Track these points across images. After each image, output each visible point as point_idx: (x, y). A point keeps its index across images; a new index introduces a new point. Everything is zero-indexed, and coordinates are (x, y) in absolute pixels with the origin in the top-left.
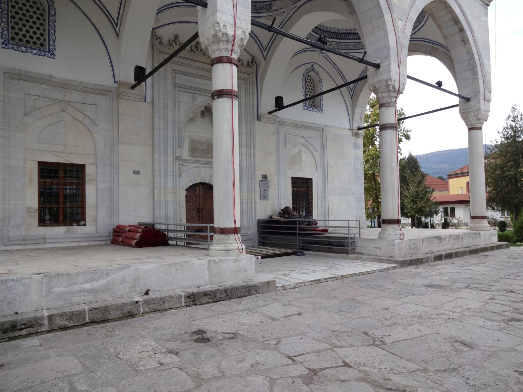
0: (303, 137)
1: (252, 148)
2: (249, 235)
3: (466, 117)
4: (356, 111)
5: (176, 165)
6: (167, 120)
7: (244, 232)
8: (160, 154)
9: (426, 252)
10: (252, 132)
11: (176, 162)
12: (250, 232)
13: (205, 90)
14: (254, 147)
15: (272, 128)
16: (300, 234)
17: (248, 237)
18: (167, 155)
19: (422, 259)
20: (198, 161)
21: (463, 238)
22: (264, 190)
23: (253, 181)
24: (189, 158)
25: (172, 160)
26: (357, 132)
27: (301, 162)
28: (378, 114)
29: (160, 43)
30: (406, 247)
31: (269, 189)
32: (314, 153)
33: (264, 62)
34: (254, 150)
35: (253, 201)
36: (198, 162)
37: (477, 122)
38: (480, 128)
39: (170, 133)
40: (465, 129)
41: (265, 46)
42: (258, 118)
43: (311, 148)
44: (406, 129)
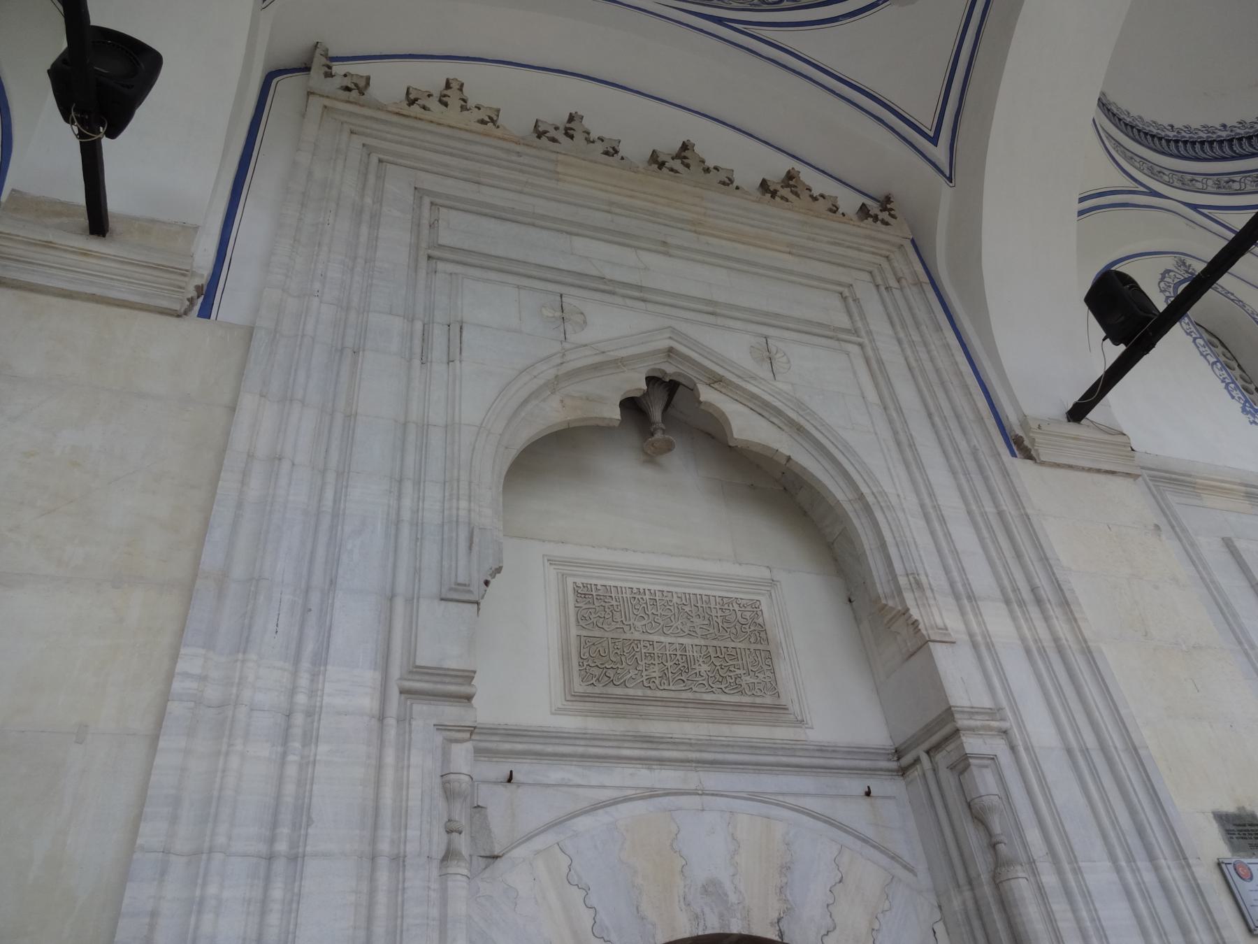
1: (1055, 612)
5: (404, 747)
6: (351, 417)
8: (243, 642)
11: (404, 720)
13: (640, 288)
18: (321, 660)
20: (649, 740)
23: (1173, 874)
24: (570, 723)
25: (368, 702)
29: (348, 89)
33: (946, 191)
34: (1072, 619)
36: (652, 752)
39: (367, 496)
41: (928, 122)
42: (1019, 446)
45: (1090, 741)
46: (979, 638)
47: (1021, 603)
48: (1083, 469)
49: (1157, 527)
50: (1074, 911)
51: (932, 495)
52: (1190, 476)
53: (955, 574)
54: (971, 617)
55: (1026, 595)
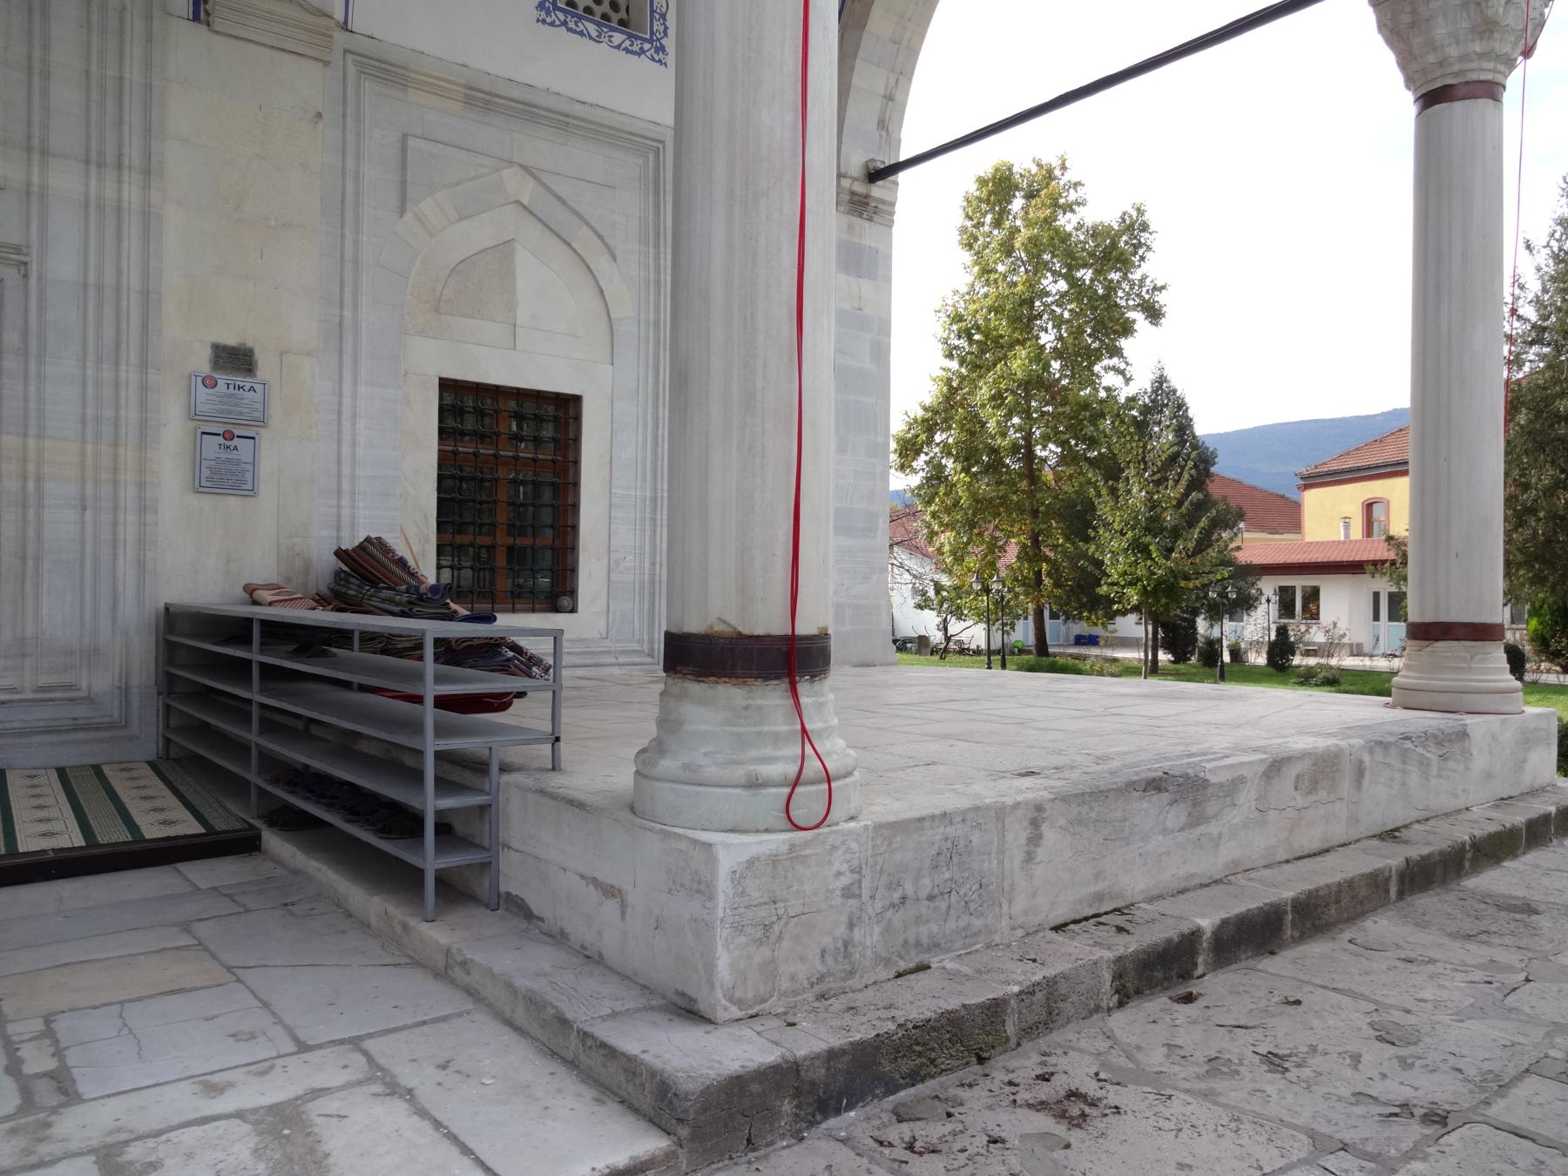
0: (525, 168)
2: (89, 700)
3: (1413, 24)
4: (856, 81)
7: (44, 680)
9: (1063, 913)
10: (134, 73)
12: (101, 682)
14: (147, 172)
15: (305, 83)
16: (263, 706)
17: (81, 712)
19: (995, 1008)
21: (1360, 771)
22: (229, 436)
23: (130, 375)
26: (860, 188)
27: (511, 305)
28: (1045, 220)
30: (848, 893)
31: (264, 435)
32: (602, 264)
34: (146, 187)
35: (129, 493)
37: (1478, 47)
38: (1491, 91)
40: (1405, 104)
43: (583, 238)
44: (1148, 281)
45: (109, 278)
46: (35, 189)
47: (100, 165)
48: (265, 45)
49: (319, 115)
50: (26, 385)
51: (46, 48)
52: (406, 69)
53: (36, 131)
54: (36, 171)
55: (110, 158)
